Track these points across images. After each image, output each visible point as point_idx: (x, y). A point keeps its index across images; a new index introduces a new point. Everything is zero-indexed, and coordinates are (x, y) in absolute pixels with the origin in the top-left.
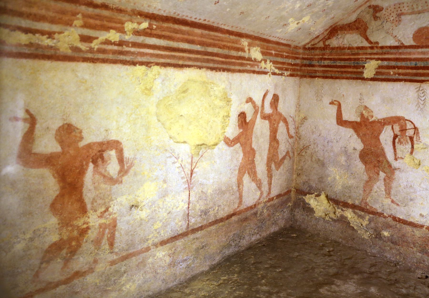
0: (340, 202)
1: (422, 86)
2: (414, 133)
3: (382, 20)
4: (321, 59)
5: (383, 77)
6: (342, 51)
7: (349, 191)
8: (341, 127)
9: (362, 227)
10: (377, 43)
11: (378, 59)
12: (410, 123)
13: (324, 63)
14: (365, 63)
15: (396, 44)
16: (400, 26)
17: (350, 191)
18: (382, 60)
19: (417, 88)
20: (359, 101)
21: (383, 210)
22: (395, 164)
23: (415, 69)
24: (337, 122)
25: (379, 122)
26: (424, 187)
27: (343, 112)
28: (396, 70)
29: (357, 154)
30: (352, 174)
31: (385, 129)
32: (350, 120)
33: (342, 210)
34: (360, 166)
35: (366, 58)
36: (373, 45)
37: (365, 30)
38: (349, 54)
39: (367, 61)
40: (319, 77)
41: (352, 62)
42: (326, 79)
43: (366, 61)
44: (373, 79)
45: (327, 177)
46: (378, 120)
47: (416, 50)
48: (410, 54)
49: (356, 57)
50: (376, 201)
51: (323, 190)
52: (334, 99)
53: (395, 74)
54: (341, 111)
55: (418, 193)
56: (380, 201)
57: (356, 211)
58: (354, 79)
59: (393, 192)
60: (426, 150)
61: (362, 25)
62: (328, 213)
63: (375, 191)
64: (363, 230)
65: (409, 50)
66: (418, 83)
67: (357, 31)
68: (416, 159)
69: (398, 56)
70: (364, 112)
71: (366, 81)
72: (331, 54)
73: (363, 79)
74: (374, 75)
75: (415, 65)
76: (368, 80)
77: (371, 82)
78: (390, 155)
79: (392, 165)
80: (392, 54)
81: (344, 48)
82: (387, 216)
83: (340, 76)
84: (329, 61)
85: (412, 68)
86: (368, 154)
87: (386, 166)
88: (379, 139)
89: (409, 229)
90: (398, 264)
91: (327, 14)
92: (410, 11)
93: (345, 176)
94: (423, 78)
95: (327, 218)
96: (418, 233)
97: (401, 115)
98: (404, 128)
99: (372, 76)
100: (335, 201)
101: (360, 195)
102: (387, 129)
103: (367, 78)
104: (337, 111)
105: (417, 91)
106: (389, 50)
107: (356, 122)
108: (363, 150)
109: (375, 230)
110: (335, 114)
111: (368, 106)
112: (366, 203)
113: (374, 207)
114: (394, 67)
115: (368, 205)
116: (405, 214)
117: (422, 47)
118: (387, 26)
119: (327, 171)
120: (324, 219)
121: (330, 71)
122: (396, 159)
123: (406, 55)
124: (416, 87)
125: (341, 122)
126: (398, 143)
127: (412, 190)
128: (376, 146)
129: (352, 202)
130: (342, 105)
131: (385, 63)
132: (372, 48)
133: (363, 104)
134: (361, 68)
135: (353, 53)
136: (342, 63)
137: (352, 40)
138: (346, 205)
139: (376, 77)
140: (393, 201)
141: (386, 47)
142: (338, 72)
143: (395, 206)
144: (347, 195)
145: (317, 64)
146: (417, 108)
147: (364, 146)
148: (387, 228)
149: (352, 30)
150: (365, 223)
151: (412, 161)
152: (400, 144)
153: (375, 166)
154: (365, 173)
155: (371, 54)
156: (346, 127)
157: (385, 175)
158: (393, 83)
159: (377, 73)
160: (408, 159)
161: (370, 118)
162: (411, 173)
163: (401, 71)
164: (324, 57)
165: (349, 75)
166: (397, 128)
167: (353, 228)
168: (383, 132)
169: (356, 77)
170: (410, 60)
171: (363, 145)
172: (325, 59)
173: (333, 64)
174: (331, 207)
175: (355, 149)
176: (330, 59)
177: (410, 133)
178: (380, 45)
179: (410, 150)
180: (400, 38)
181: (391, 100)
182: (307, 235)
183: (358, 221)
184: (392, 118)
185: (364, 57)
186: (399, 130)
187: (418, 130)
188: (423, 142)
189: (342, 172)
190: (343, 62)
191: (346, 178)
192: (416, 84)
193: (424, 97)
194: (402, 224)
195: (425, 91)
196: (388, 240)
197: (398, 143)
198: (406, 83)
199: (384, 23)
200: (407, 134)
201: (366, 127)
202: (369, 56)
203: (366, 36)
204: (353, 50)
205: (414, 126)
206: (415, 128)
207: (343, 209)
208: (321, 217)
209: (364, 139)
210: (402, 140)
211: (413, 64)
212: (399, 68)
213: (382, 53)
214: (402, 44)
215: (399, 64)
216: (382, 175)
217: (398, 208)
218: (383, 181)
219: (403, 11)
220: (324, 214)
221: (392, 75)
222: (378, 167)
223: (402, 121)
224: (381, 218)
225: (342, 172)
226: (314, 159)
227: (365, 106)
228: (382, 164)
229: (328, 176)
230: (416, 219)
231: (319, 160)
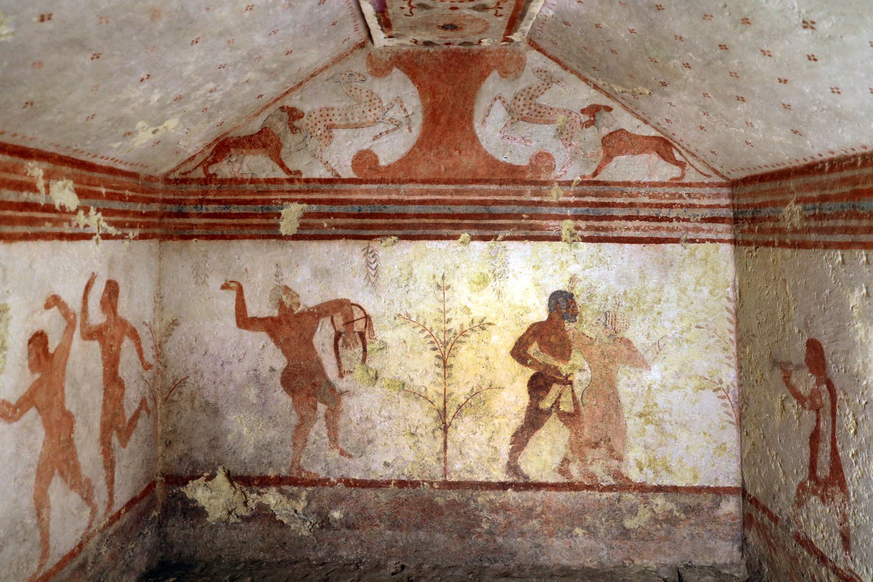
3: (304, 134)
5: (313, 232)
10: (299, 172)
11: (302, 201)
15: (329, 175)
16: (332, 145)
18: (310, 202)
26: (386, 414)
28: (332, 220)
29: (277, 379)
32: (260, 316)
34: (283, 399)
35: (282, 199)
36: (292, 176)
37: (278, 148)
38: (252, 193)
44: (296, 237)
46: (309, 310)
49: (265, 197)
53: (330, 226)
54: (243, 300)
55: (378, 428)
58: (263, 237)
59: (341, 436)
61: (271, 140)
63: (312, 441)
65: (348, 186)
67: (264, 150)
68: (372, 369)
69: (332, 196)
70: (284, 297)
73: (280, 237)
74: (298, 228)
75: (360, 210)
76: (289, 239)
77: (293, 243)
78: (331, 371)
80: (323, 192)
81: (243, 181)
85: (354, 216)
86: (296, 375)
87: (327, 391)
88: (312, 345)
90: (361, 562)
91: (210, 117)
92: (343, 123)
99: (295, 232)
103: (286, 236)
104: (237, 300)
106: (318, 185)
107: (272, 318)
108: (286, 369)
109: (319, 514)
111: (290, 287)
112: (299, 467)
114: (328, 215)
117: (366, 182)
118: (313, 143)
122: (341, 376)
127: (369, 425)
128: (308, 358)
131: (314, 208)
132: (291, 181)
133: (282, 283)
136: (242, 209)
137: (255, 165)
139: (301, 232)
140: (342, 453)
141: (314, 180)
142: (234, 225)
144: (265, 461)
147: (289, 361)
149: (255, 148)
153: (308, 395)
154: (294, 412)
155: (290, 192)
156: (255, 330)
158: (328, 241)
159: (302, 226)
161: (294, 308)
162: (365, 395)
163: (339, 221)
165: (254, 232)
168: (319, 330)
175: (272, 370)
178: (304, 177)
179: (361, 356)
180: (333, 165)
181: (327, 271)
182: (198, 570)
183: (288, 506)
185: (279, 197)
198: (348, 241)
199: (308, 140)
201: (288, 325)
203: (281, 160)
208: (220, 519)
209: (287, 348)
211: (355, 209)
212: (336, 215)
214: (337, 175)
215: (336, 209)
216: (322, 408)
217: (351, 461)
218: (323, 418)
219: (334, 122)
222: (314, 395)
227: (286, 286)
230: (380, 473)
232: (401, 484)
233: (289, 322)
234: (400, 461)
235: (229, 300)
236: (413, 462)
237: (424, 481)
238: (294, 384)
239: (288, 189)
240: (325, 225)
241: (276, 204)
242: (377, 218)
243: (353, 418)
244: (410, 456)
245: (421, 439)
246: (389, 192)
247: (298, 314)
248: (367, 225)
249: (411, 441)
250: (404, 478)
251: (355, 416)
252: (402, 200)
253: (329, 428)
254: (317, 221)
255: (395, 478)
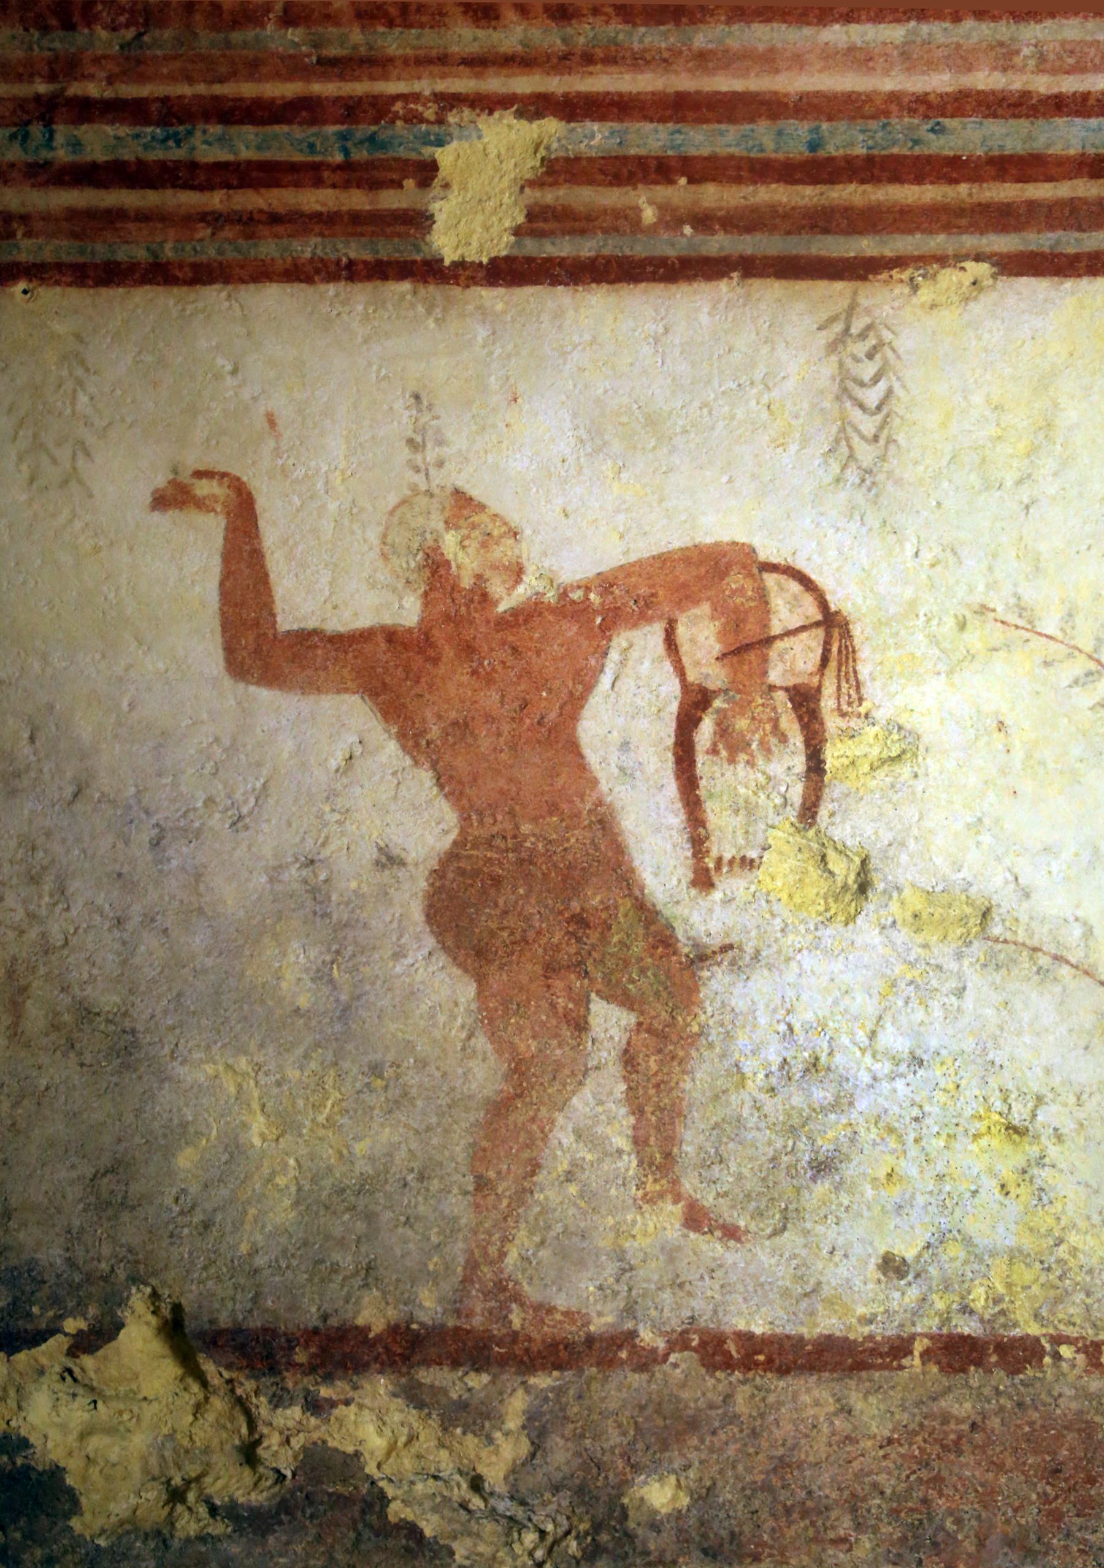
0: (291, 1344)
1: (863, 302)
2: (825, 661)
4: (47, 110)
5: (587, 248)
6: (236, 36)
7: (361, 1226)
8: (264, 694)
9: (476, 1502)
11: (536, 107)
12: (795, 587)
13: (76, 145)
14: (440, 143)
17: (370, 1217)
18: (572, 108)
19: (833, 319)
20: (406, 453)
21: (630, 1310)
22: (696, 918)
23: (815, 182)
24: (229, 650)
25: (569, 607)
27: (276, 564)
28: (680, 193)
30: (376, 1069)
31: (614, 655)
32: (337, 623)
33: (315, 1406)
35: (438, 97)
39: (452, 118)
40: (36, 272)
41: (331, 129)
42: (106, 292)
43: (440, 121)
44: (506, 272)
45: (168, 1153)
47: (808, 31)
48: (769, 60)
49: (359, 88)
50: (572, 1250)
51: (135, 1279)
52: (193, 460)
53: (672, 219)
55: (862, 1104)
56: (604, 1243)
57: (427, 1376)
58: (351, 272)
59: (692, 1141)
60: (905, 771)
62: (193, 1470)
64: (489, 1527)
66: (839, 285)
68: (842, 851)
69: (683, 82)
70: (450, 542)
71: (456, 291)
72: (132, 63)
73: (432, 272)
74: (517, 232)
75: (813, 146)
76: (472, 281)
77: (493, 297)
78: (657, 859)
79: (680, 934)
80: (639, 61)
82: (661, 1344)
83: (230, 255)
84: (123, 130)
86: (497, 881)
87: (638, 948)
88: (574, 747)
89: (811, 1397)
93: (317, 1107)
94: (866, 246)
95: (188, 1525)
96: (874, 1409)
97: (725, 537)
98: (751, 630)
99: (502, 245)
100: (247, 1350)
101: (451, 1228)
102: (634, 654)
103: (460, 264)
104: (229, 556)
105: (833, 347)
106: (616, 29)
107: (391, 635)
108: (452, 856)
110: (206, 589)
111: (475, 493)
113: (561, 1302)
114: (660, 170)
115: (517, 1298)
116: (785, 1293)
119: (166, 1096)
120: (161, 1536)
121: (143, 217)
122: (703, 881)
123: (745, 74)
124: (825, 316)
125: (260, 645)
126: (714, 751)
127: (821, 1095)
128: (553, 808)
129: (393, 1314)
130: (261, 503)
131: (596, 137)
133: (438, 478)
134: (409, 183)
135: (333, 51)
136: (246, 144)
138: (341, 1352)
139: (530, 247)
140: (696, 1218)
142: (214, 220)
143: (711, 1247)
145: (14, 154)
146: (836, 468)
147: (465, 819)
148: (665, 1447)
150: (500, 1457)
151: (814, 873)
152: (732, 761)
153: (550, 969)
154: (481, 1042)
156: (311, 687)
157: (629, 1019)
158: (658, 290)
159: (538, 221)
160: (783, 863)
161: (496, 587)
163: (713, 196)
164: (75, 89)
165: (307, 248)
166: (702, 635)
167: (413, 1531)
168: (606, 680)
169: (368, 256)
170: (773, 107)
171: (451, 817)
172: (87, 110)
173: (157, 154)
174: (218, 1404)
175: (389, 860)
176: (135, 111)
177: (795, 659)
181: (652, 421)
184: (663, 560)
185: (425, 86)
186: (717, 648)
187: (846, 634)
188: (880, 715)
189: (293, 1074)
190: (249, 131)
191: (330, 1123)
192: (822, 288)
193: (882, 385)
194: (771, 1380)
195: (887, 336)
196: (683, 1538)
197: (714, 751)
198: (756, 283)
200: (775, 676)
201: (469, 667)
202: (462, 84)
204: (332, 31)
205: (823, 605)
206: (832, 623)
207: (325, 1392)
209: (460, 763)
210: (742, 724)
211: (794, 139)
212: (698, 170)
213: (566, 57)
215: (699, 140)
216: (610, 1022)
217: (732, 1256)
220: (154, 1494)
221: (653, 229)
222: (579, 967)
223: (735, 580)
224: (617, 1377)
225: (293, 1074)
226: (35, 1015)
227: (458, 493)
228: (604, 939)
229: (182, 1133)
230: (860, 1304)
231: (86, 1013)
232: (957, 1353)
233: (468, 650)
234: (955, 1251)
235: (193, 554)
236: (1015, 1255)
237: (1058, 1340)
238: (487, 919)
239: (473, 49)
240: (649, 215)
241: (414, 118)
242: (896, 179)
243: (749, 1066)
244: (994, 1224)
245: (1054, 1152)
246: (962, 59)
247: (515, 612)
248: (847, 211)
249: (1009, 1159)
250: (967, 1327)
251: (759, 1050)
252: (1026, 95)
253: (638, 1111)
254: (611, 197)
255: (929, 1324)
